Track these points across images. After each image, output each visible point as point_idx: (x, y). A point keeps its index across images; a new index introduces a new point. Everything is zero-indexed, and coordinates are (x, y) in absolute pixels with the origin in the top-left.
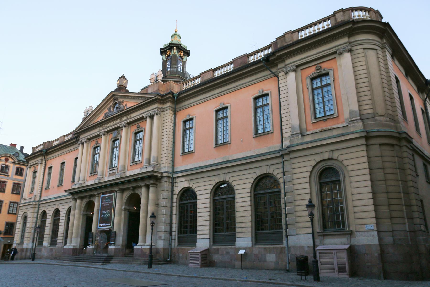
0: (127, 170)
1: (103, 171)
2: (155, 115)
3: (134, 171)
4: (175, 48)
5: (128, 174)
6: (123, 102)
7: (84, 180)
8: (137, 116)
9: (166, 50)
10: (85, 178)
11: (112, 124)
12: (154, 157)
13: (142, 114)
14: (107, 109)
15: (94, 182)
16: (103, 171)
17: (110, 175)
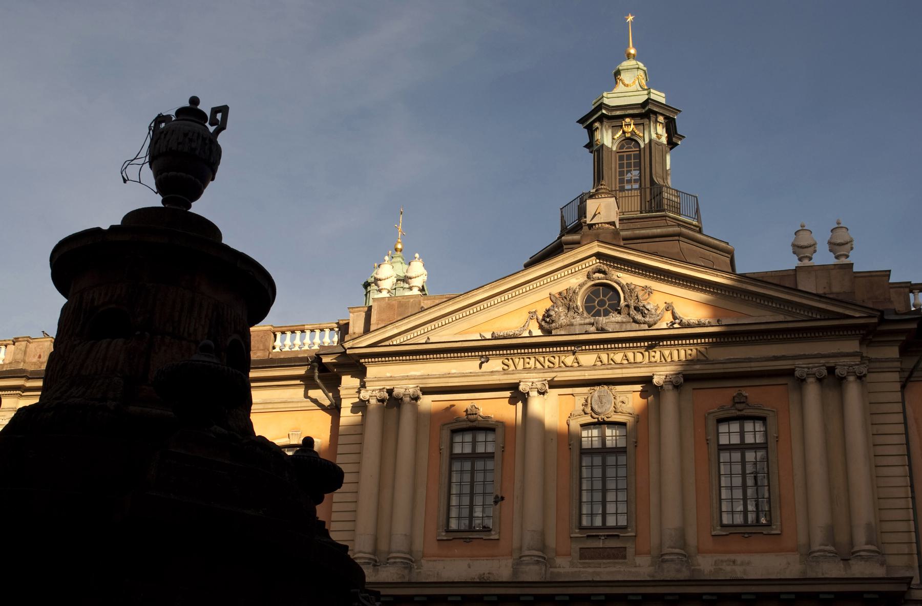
0: (699, 551)
1: (543, 534)
2: (851, 378)
3: (739, 558)
4: (661, 119)
5: (706, 565)
6: (649, 291)
7: (410, 552)
8: (750, 360)
9: (623, 117)
10: (411, 543)
11: (587, 359)
12: (869, 526)
13: (776, 358)
14: (545, 294)
15: (515, 572)
16: (543, 534)
17: (585, 554)
